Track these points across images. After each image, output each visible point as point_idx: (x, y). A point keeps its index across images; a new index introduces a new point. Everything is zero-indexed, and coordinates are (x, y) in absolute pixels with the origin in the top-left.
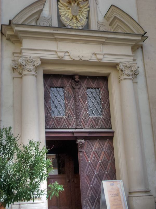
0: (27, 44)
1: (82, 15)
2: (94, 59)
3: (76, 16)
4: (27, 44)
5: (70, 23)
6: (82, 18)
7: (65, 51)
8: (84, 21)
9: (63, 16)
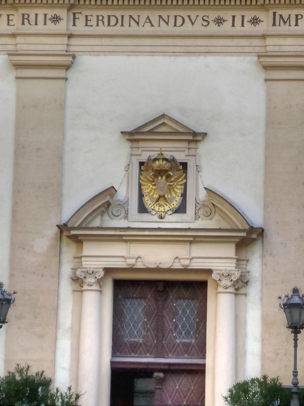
1: (174, 191)
2: (177, 266)
3: (164, 196)
4: (89, 249)
5: (155, 207)
6: (174, 195)
7: (137, 256)
8: (176, 201)
9: (147, 196)
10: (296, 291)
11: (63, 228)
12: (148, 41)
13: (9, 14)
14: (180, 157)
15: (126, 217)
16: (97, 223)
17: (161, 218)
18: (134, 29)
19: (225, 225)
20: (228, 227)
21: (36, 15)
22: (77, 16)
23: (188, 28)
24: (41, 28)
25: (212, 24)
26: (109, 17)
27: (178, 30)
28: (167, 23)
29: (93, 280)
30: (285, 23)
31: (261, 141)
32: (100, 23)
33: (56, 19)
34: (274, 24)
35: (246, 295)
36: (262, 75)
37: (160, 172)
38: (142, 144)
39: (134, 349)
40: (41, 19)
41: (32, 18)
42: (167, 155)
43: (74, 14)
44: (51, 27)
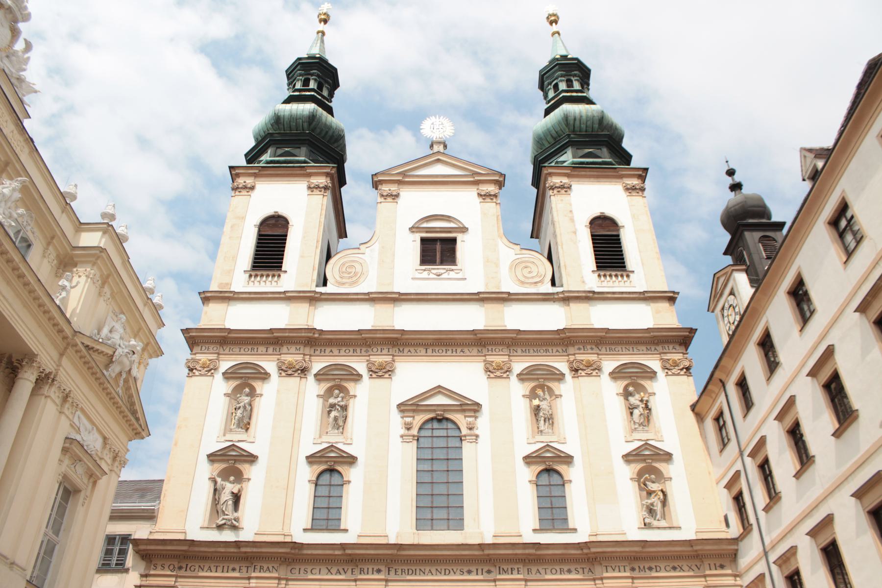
13: (353, 567)
21: (368, 569)
22: (390, 569)
25: (465, 573)
26: (408, 570)
30: (505, 572)
32: (403, 573)
33: (379, 571)
40: (370, 570)
43: (389, 568)
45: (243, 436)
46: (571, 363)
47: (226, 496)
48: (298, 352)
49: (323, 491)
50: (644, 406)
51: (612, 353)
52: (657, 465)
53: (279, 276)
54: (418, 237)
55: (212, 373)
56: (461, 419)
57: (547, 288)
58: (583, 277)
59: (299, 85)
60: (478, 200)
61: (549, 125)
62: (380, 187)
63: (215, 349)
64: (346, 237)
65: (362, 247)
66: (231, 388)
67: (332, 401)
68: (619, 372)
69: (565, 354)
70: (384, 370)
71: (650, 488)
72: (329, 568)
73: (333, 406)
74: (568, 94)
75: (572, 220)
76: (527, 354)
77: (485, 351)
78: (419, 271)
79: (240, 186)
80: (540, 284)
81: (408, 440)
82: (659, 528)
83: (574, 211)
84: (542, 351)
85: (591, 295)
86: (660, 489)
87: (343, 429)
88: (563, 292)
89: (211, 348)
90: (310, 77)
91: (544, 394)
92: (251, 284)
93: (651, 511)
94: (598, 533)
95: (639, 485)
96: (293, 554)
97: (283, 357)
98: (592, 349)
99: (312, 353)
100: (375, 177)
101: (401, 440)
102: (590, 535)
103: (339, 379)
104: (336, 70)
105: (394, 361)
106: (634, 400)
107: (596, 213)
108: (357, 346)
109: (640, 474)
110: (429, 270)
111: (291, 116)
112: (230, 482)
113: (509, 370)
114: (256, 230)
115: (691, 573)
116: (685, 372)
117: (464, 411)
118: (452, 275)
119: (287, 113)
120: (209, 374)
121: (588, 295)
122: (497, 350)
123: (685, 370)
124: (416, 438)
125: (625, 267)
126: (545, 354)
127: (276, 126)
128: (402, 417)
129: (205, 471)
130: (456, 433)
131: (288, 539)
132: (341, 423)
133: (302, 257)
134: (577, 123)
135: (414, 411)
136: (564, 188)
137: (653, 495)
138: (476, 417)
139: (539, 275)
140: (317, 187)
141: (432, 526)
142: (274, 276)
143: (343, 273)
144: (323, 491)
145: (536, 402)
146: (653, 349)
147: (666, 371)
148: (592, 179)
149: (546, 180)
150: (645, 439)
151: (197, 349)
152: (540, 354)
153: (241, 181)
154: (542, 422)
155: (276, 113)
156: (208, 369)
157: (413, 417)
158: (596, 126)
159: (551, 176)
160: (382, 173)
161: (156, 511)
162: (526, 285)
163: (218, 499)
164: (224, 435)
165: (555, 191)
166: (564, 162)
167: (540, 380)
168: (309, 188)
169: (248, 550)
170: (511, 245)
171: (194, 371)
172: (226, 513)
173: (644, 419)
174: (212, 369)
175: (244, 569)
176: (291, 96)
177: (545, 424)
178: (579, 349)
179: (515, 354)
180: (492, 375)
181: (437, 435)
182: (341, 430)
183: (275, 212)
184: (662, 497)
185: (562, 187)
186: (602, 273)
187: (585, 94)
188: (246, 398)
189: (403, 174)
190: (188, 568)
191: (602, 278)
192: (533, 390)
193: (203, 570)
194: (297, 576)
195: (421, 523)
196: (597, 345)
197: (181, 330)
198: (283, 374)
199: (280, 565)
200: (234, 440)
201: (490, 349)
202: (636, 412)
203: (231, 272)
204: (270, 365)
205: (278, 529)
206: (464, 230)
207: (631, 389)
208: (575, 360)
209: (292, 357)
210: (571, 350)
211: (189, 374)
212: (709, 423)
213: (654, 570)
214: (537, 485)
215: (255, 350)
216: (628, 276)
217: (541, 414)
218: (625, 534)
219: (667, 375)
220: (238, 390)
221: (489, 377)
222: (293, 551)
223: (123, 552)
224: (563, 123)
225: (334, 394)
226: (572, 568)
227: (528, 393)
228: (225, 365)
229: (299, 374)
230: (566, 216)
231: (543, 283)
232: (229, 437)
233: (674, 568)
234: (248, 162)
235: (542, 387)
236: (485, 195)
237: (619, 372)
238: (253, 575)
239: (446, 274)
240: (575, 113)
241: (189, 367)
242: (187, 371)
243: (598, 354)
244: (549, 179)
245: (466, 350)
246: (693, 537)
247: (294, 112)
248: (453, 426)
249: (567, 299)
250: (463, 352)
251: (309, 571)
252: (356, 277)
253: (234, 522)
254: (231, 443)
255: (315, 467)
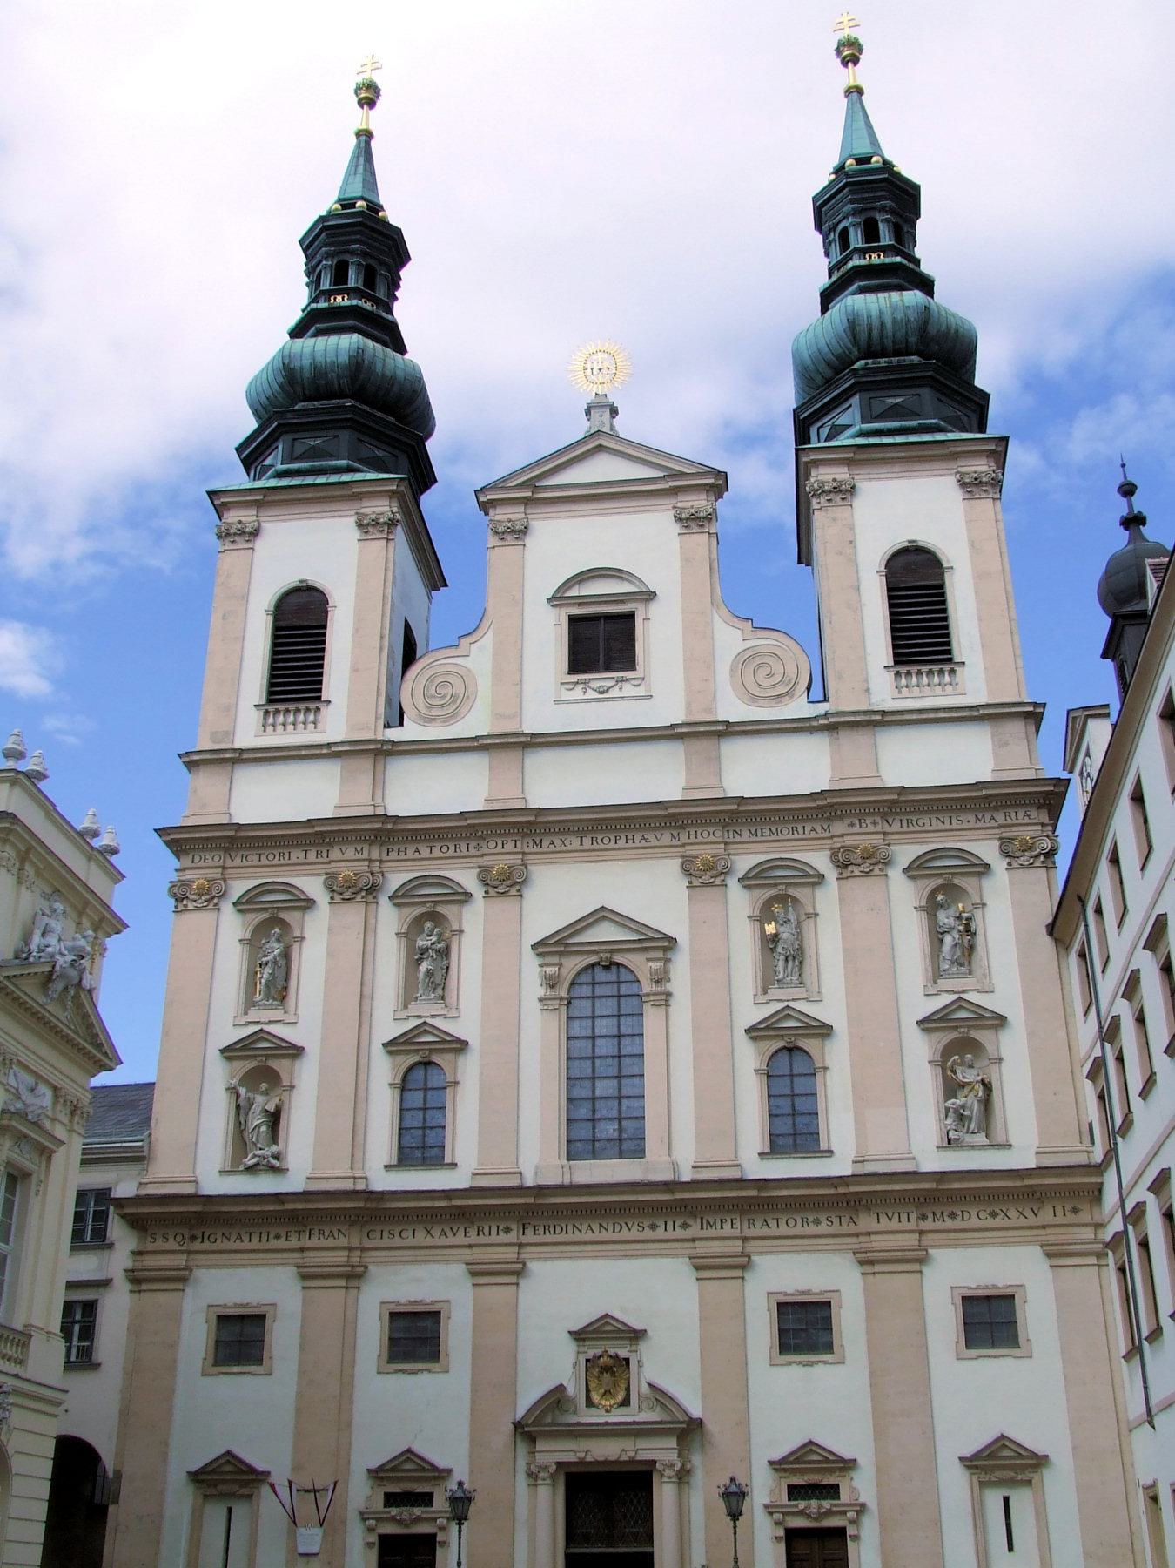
0: (540, 1446)
2: (624, 1458)
10: (733, 1480)
11: (518, 1425)
12: (590, 1247)
14: (623, 1353)
15: (575, 1412)
16: (549, 1419)
17: (607, 1411)
18: (578, 1237)
19: (666, 1417)
20: (669, 1419)
23: (625, 1234)
24: (494, 1238)
25: (646, 1229)
27: (616, 1237)
28: (607, 1230)
29: (547, 1475)
31: (696, 1335)
33: (507, 1230)
34: (702, 1228)
35: (688, 1483)
36: (694, 1274)
37: (606, 1369)
38: (587, 1343)
39: (587, 1540)
40: (494, 1230)
41: (486, 1230)
42: (611, 1352)
44: (503, 1238)
45: (277, 1014)
46: (834, 853)
47: (256, 1120)
48: (359, 856)
49: (416, 1098)
50: (961, 928)
51: (911, 828)
52: (975, 1034)
53: (318, 709)
54: (562, 616)
55: (216, 905)
56: (640, 964)
57: (799, 708)
58: (867, 681)
59: (326, 284)
60: (676, 528)
61: (822, 343)
62: (492, 512)
63: (217, 858)
64: (446, 585)
65: (464, 642)
66: (251, 928)
67: (420, 943)
68: (919, 867)
69: (827, 834)
70: (509, 882)
71: (961, 1077)
72: (429, 1227)
73: (424, 951)
74: (863, 262)
75: (853, 561)
76: (759, 838)
77: (684, 838)
78: (567, 686)
79: (232, 531)
80: (787, 698)
81: (551, 1007)
82: (973, 1147)
83: (860, 542)
84: (785, 831)
85: (878, 717)
86: (979, 1078)
87: (443, 989)
88: (826, 715)
89: (209, 858)
90: (346, 257)
91: (786, 912)
92: (270, 729)
93: (961, 1118)
94: (866, 1158)
95: (944, 1069)
96: (367, 1209)
97: (333, 868)
98: (874, 823)
99: (384, 857)
100: (479, 495)
101: (538, 1006)
102: (855, 1162)
103: (432, 902)
104: (398, 232)
105: (525, 866)
106: (944, 918)
107: (900, 540)
108: (461, 839)
109: (947, 1052)
110: (585, 682)
111: (316, 367)
112: (262, 1093)
113: (726, 872)
114: (271, 618)
115: (1023, 1222)
116: (1043, 862)
117: (646, 949)
118: (628, 689)
119: (306, 362)
120: (211, 906)
121: (874, 717)
122: (705, 834)
123: (1042, 858)
124: (566, 1002)
125: (949, 652)
126: (790, 836)
127: (289, 388)
128: (541, 966)
129: (218, 1076)
130: (634, 989)
131: (361, 1186)
132: (438, 978)
133: (355, 670)
134: (875, 332)
135: (561, 954)
136: (840, 491)
137: (966, 1090)
138: (668, 961)
139: (787, 679)
140: (375, 523)
141: (593, 1152)
142: (308, 710)
143: (431, 697)
144: (416, 1098)
145: (770, 929)
146: (988, 817)
147: (1008, 860)
148: (897, 468)
149: (807, 478)
150: (961, 989)
151: (187, 861)
152: (781, 837)
153: (232, 517)
154: (781, 964)
155: (286, 361)
156: (208, 897)
157: (560, 965)
158: (913, 340)
159: (817, 467)
160: (494, 487)
161: (146, 1149)
162: (762, 703)
163: (243, 1122)
164: (246, 1013)
165: (823, 500)
166: (847, 427)
167: (780, 887)
168: (360, 525)
169: (299, 1206)
170: (736, 622)
171: (185, 902)
172: (259, 1145)
173: (963, 952)
174: (213, 898)
175: (294, 1237)
176: (312, 310)
177: (786, 968)
178: (852, 825)
179: (738, 839)
180: (696, 882)
181: (602, 994)
182: (439, 991)
183: (301, 581)
184: (980, 1094)
185: (837, 490)
186: (903, 669)
187: (898, 259)
188: (276, 945)
189: (530, 484)
190: (206, 1238)
191: (903, 681)
192: (768, 904)
193: (229, 1240)
194: (377, 1243)
195: (575, 1149)
196: (885, 816)
197: (155, 830)
198: (338, 898)
199: (350, 1226)
200: (262, 1020)
201: (692, 832)
202: (948, 940)
203: (231, 710)
204: (312, 886)
205: (343, 1168)
206: (649, 596)
207: (940, 897)
208: (842, 847)
209: (350, 862)
210: (839, 827)
211: (176, 907)
212: (1073, 958)
213: (960, 1218)
214: (768, 1076)
215: (286, 856)
216: (952, 671)
217: (780, 949)
218: (914, 1159)
219: (1010, 868)
220: (261, 930)
221: (690, 886)
222: (368, 1206)
223: (101, 1217)
224: (846, 340)
225: (426, 929)
226: (823, 1218)
227: (757, 913)
228: (239, 888)
229: (363, 897)
230: (841, 553)
231: (792, 697)
232: (254, 1015)
233: (994, 1215)
234: (248, 463)
235: (783, 899)
236: (687, 519)
237: (919, 867)
238: (309, 1244)
239: (617, 688)
240: (869, 316)
241: (174, 896)
242: (173, 901)
243: (885, 834)
244: (814, 473)
245: (651, 837)
246: (1031, 1162)
247: (319, 359)
248: (630, 977)
249: (832, 726)
250: (646, 840)
251: (397, 1234)
252: (455, 705)
253: (273, 1162)
254: (257, 1028)
255: (400, 1058)
